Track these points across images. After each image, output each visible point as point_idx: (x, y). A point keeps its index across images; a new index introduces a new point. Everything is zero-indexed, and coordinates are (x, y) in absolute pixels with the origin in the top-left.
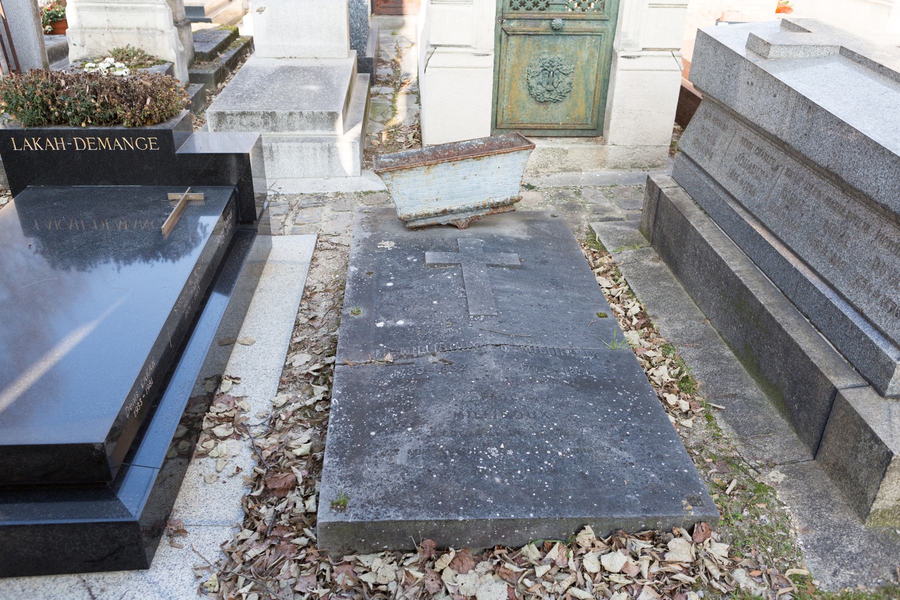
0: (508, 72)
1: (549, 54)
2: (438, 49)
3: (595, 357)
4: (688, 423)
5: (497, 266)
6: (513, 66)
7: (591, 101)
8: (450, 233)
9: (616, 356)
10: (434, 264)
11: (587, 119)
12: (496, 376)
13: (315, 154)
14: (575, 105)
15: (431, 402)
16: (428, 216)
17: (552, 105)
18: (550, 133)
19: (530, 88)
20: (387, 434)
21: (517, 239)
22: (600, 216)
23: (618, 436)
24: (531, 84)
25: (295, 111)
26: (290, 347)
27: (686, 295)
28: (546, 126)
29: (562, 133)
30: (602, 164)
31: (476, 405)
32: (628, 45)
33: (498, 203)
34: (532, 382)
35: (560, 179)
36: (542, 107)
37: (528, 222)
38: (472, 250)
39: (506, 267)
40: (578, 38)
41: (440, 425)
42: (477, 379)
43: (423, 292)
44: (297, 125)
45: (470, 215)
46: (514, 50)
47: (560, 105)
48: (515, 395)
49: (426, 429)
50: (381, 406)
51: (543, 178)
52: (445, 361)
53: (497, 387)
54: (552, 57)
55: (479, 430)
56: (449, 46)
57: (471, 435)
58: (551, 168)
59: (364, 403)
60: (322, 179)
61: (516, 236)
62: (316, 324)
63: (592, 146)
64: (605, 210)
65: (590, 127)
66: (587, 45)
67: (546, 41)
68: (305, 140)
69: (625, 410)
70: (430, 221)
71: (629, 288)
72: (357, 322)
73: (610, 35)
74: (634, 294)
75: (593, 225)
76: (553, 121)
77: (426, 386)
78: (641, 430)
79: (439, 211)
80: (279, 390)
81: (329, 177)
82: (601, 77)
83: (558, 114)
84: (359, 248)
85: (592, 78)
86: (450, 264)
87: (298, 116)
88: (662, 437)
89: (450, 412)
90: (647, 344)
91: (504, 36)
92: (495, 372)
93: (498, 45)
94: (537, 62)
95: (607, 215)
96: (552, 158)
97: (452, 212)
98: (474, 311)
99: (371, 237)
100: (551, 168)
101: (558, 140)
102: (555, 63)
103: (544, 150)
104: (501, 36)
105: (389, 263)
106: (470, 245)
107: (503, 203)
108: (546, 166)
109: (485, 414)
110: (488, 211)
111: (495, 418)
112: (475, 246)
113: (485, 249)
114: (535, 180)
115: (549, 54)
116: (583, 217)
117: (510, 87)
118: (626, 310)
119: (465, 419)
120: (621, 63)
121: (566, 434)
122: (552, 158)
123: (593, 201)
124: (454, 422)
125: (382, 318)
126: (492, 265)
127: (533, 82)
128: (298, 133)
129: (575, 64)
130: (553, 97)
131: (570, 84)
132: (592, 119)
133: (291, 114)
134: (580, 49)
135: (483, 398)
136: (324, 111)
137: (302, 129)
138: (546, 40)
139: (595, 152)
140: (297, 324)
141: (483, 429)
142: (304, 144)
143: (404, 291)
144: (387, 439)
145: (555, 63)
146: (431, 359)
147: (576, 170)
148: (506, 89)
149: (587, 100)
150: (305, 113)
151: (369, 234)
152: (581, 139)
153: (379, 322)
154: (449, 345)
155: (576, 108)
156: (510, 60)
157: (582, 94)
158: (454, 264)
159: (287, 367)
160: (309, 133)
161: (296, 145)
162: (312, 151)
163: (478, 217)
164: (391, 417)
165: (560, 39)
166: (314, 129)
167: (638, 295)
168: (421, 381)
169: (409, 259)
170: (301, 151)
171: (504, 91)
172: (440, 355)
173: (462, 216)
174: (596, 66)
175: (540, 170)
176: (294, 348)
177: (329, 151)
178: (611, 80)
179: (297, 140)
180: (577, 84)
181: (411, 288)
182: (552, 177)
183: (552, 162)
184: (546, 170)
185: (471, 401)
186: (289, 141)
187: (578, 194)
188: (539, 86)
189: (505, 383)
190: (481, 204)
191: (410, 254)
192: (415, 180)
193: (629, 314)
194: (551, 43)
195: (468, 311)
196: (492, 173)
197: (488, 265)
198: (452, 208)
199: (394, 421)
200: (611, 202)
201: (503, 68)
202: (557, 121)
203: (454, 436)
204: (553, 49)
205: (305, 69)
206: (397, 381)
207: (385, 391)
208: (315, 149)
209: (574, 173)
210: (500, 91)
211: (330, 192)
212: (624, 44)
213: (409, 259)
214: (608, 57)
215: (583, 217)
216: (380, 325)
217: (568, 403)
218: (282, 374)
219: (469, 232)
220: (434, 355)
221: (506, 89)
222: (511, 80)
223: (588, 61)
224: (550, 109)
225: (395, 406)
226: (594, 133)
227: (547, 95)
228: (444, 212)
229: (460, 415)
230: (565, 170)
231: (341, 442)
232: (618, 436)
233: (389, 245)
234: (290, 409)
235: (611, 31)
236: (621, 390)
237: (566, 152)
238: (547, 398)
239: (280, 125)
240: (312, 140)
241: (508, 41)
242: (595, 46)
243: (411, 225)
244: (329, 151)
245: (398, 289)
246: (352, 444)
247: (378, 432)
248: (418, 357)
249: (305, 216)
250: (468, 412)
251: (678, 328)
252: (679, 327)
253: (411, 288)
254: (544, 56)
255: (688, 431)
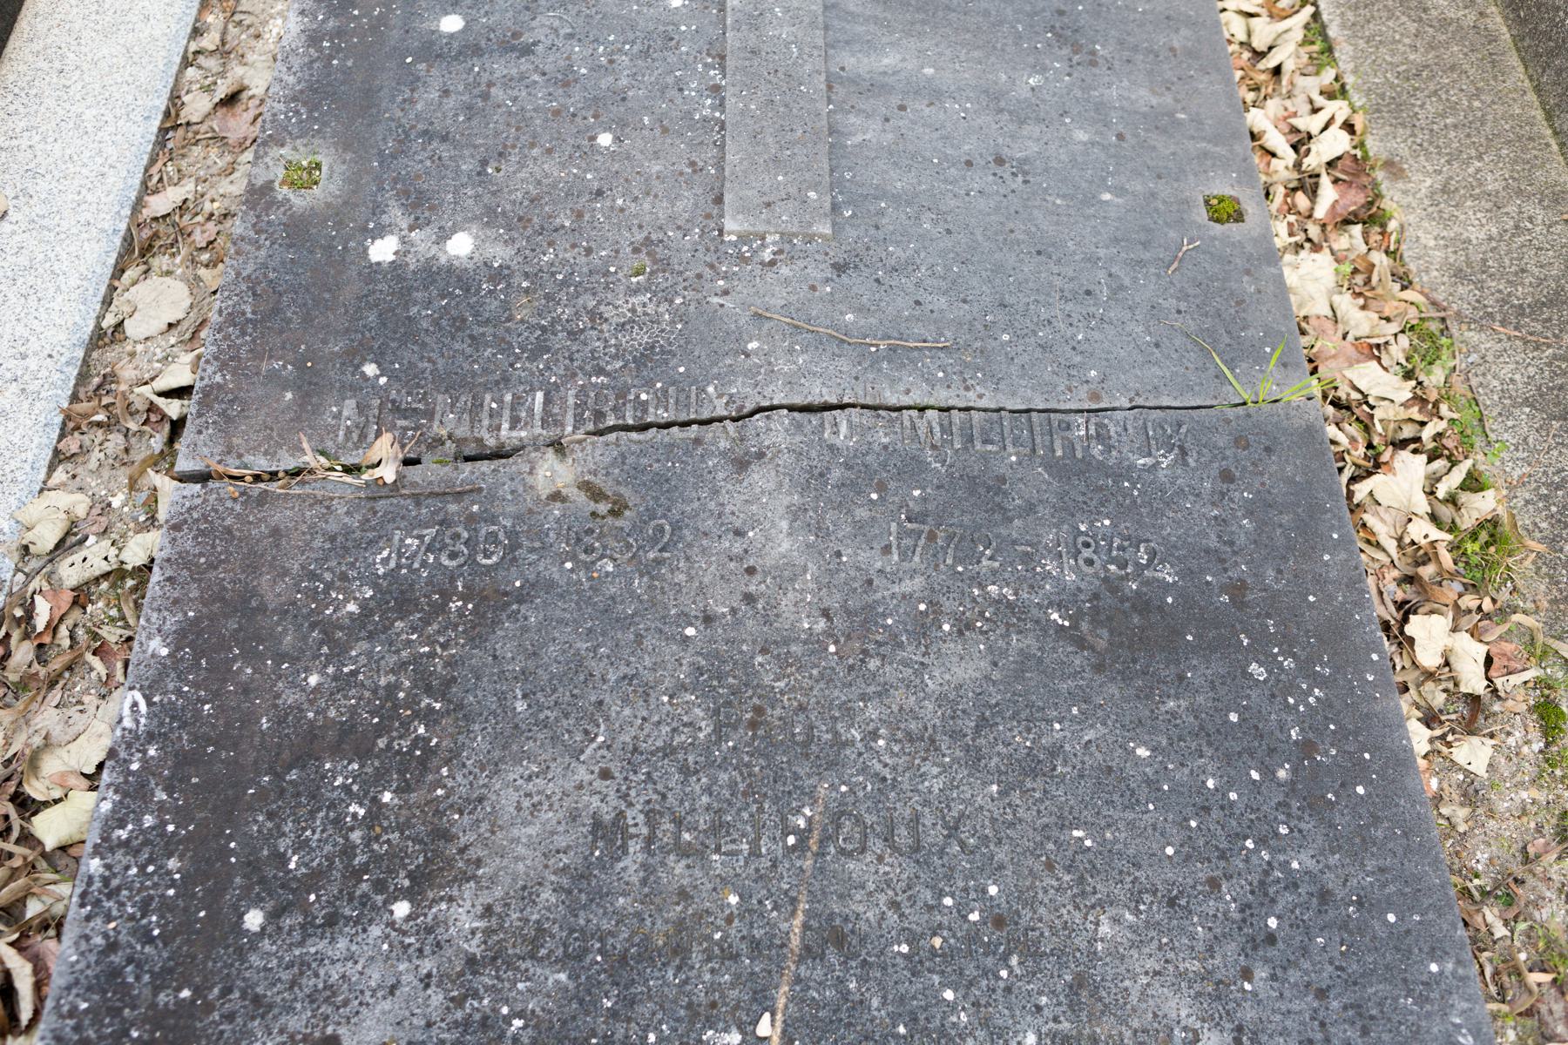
3: (1184, 452)
4: (1473, 754)
9: (1259, 437)
12: (786, 603)
15: (510, 737)
20: (308, 930)
23: (1231, 948)
26: (128, 239)
27: (1517, 73)
31: (685, 771)
34: (923, 629)
41: (527, 895)
42: (708, 619)
43: (566, 80)
48: (848, 711)
49: (463, 918)
50: (309, 745)
52: (596, 494)
53: (784, 662)
55: (680, 925)
57: (647, 954)
59: (250, 719)
62: (239, 125)
69: (1268, 772)
71: (1316, 16)
72: (298, 229)
74: (1329, 50)
77: (505, 638)
78: (1324, 896)
80: (58, 457)
88: (1400, 938)
89: (574, 817)
90: (1361, 322)
92: (786, 575)
98: (744, 209)
109: (718, 828)
111: (755, 853)
118: (1301, 142)
119: (631, 863)
121: (1031, 952)
124: (582, 876)
125: (396, 214)
135: (719, 734)
140: (171, 121)
141: (699, 916)
143: (500, 67)
144: (304, 964)
146: (552, 474)
153: (380, 232)
154: (622, 394)
159: (106, 337)
164: (337, 822)
167: (1344, 52)
168: (492, 602)
172: (594, 455)
176: (140, 248)
181: (527, 50)
185: (668, 751)
189: (815, 644)
193: (1312, 162)
195: (719, 200)
199: (348, 851)
203: (572, 959)
206: (398, 598)
207: (339, 652)
216: (383, 250)
217: (1055, 751)
218: (83, 377)
220: (558, 446)
225: (364, 753)
229: (609, 833)
231: (115, 973)
232: (1231, 948)
234: (71, 572)
236: (1260, 651)
238: (970, 729)
245: (477, 51)
246: (161, 980)
247: (274, 916)
248: (499, 454)
250: (651, 816)
251: (1475, 234)
252: (1477, 228)
253: (527, 50)
255: (1471, 793)
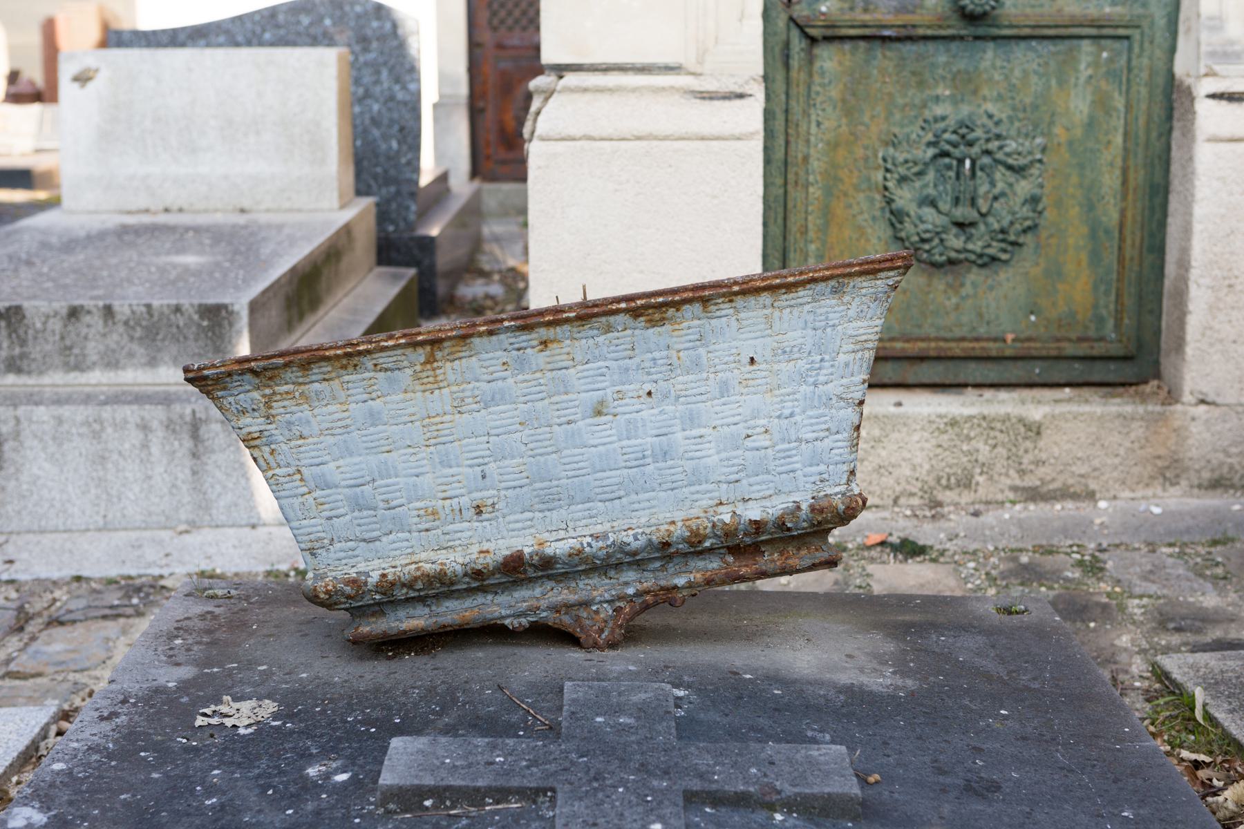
0: (815, 164)
1: (955, 101)
2: (571, 79)
5: (741, 801)
6: (834, 146)
7: (1110, 258)
8: (536, 664)
10: (422, 792)
11: (1100, 321)
13: (145, 446)
14: (1055, 273)
16: (438, 587)
17: (974, 276)
18: (974, 371)
19: (897, 217)
21: (849, 690)
22: (1190, 637)
24: (899, 203)
25: (87, 303)
28: (957, 349)
29: (1016, 372)
30: (1169, 471)
32: (1227, 55)
33: (758, 526)
35: (1020, 523)
36: (940, 283)
37: (900, 631)
38: (625, 729)
39: (789, 805)
40: (1050, 47)
44: (93, 349)
45: (632, 582)
46: (834, 93)
47: (1004, 275)
51: (958, 521)
54: (965, 110)
56: (606, 69)
58: (984, 488)
60: (165, 535)
61: (844, 678)
63: (1128, 409)
64: (1205, 619)
65: (1115, 349)
66: (1084, 71)
67: (942, 59)
68: (117, 398)
70: (454, 612)
73: (1160, 36)
75: (1170, 663)
76: (982, 330)
79: (490, 560)
81: (193, 526)
82: (1138, 177)
83: (994, 304)
84: (106, 727)
85: (1110, 181)
86: (501, 794)
87: (96, 321)
91: (797, 43)
93: (780, 76)
94: (914, 131)
95: (1216, 633)
96: (984, 451)
97: (545, 568)
99: (184, 686)
100: (984, 488)
101: (1003, 395)
102: (979, 133)
103: (954, 423)
104: (787, 45)
105: (210, 791)
106: (619, 710)
107: (780, 524)
108: (966, 483)
110: (713, 565)
112: (642, 711)
113: (688, 729)
114: (928, 527)
115: (955, 101)
116: (1124, 640)
117: (827, 213)
120: (1210, 117)
122: (984, 451)
123: (1153, 588)
126: (717, 799)
127: (905, 197)
128: (97, 377)
129: (1047, 134)
130: (977, 246)
131: (1034, 200)
132: (1118, 326)
133: (74, 313)
134: (1062, 83)
136: (185, 302)
137: (111, 362)
138: (940, 56)
139: (1138, 430)
142: (107, 412)
145: (979, 133)
147: (1075, 497)
148: (813, 221)
149: (1095, 257)
150: (122, 308)
151: (187, 672)
152: (1086, 392)
155: (1060, 283)
156: (822, 124)
157: (1076, 236)
158: (521, 793)
160: (133, 376)
161: (82, 413)
162: (135, 437)
163: (667, 597)
165: (989, 55)
166: (152, 362)
169: (312, 771)
170: (96, 435)
171: (804, 231)
173: (599, 589)
174: (1119, 140)
175: (947, 496)
177: (195, 435)
178: (1176, 184)
179: (87, 399)
180: (1059, 204)
182: (989, 518)
183: (986, 468)
184: (966, 498)
186: (59, 401)
187: (1094, 568)
188: (928, 212)
190: (679, 531)
191: (326, 753)
192: (374, 418)
194: (961, 65)
196: (724, 389)
197: (692, 799)
198: (549, 550)
200: (1222, 592)
201: (798, 149)
202: (995, 331)
204: (966, 84)
205: (197, 230)
208: (144, 427)
209: (1070, 505)
210: (794, 228)
211: (180, 570)
212: (1213, 54)
213: (312, 771)
214: (1158, 111)
215: (1124, 640)
219: (622, 662)
221: (813, 221)
222: (828, 192)
223: (1091, 124)
224: (968, 289)
226: (1128, 372)
227: (955, 241)
228: (515, 570)
230: (1033, 495)
233: (243, 714)
235: (1161, 22)
237: (1035, 430)
239: (35, 351)
240: (140, 399)
241: (811, 60)
242: (1112, 75)
243: (371, 627)
244: (195, 435)
249: (57, 647)
254: (939, 110)
